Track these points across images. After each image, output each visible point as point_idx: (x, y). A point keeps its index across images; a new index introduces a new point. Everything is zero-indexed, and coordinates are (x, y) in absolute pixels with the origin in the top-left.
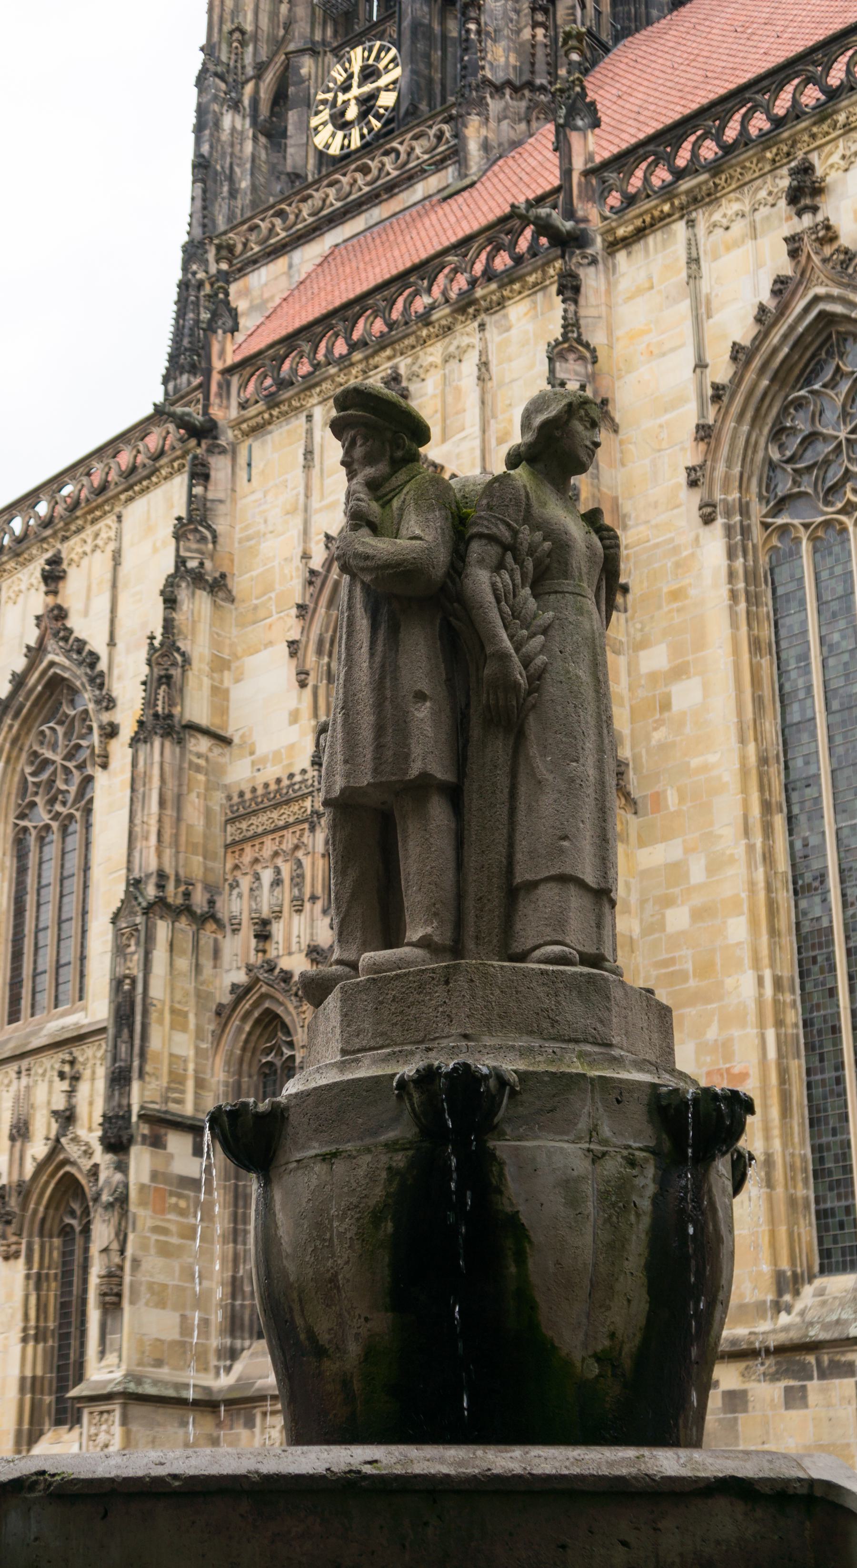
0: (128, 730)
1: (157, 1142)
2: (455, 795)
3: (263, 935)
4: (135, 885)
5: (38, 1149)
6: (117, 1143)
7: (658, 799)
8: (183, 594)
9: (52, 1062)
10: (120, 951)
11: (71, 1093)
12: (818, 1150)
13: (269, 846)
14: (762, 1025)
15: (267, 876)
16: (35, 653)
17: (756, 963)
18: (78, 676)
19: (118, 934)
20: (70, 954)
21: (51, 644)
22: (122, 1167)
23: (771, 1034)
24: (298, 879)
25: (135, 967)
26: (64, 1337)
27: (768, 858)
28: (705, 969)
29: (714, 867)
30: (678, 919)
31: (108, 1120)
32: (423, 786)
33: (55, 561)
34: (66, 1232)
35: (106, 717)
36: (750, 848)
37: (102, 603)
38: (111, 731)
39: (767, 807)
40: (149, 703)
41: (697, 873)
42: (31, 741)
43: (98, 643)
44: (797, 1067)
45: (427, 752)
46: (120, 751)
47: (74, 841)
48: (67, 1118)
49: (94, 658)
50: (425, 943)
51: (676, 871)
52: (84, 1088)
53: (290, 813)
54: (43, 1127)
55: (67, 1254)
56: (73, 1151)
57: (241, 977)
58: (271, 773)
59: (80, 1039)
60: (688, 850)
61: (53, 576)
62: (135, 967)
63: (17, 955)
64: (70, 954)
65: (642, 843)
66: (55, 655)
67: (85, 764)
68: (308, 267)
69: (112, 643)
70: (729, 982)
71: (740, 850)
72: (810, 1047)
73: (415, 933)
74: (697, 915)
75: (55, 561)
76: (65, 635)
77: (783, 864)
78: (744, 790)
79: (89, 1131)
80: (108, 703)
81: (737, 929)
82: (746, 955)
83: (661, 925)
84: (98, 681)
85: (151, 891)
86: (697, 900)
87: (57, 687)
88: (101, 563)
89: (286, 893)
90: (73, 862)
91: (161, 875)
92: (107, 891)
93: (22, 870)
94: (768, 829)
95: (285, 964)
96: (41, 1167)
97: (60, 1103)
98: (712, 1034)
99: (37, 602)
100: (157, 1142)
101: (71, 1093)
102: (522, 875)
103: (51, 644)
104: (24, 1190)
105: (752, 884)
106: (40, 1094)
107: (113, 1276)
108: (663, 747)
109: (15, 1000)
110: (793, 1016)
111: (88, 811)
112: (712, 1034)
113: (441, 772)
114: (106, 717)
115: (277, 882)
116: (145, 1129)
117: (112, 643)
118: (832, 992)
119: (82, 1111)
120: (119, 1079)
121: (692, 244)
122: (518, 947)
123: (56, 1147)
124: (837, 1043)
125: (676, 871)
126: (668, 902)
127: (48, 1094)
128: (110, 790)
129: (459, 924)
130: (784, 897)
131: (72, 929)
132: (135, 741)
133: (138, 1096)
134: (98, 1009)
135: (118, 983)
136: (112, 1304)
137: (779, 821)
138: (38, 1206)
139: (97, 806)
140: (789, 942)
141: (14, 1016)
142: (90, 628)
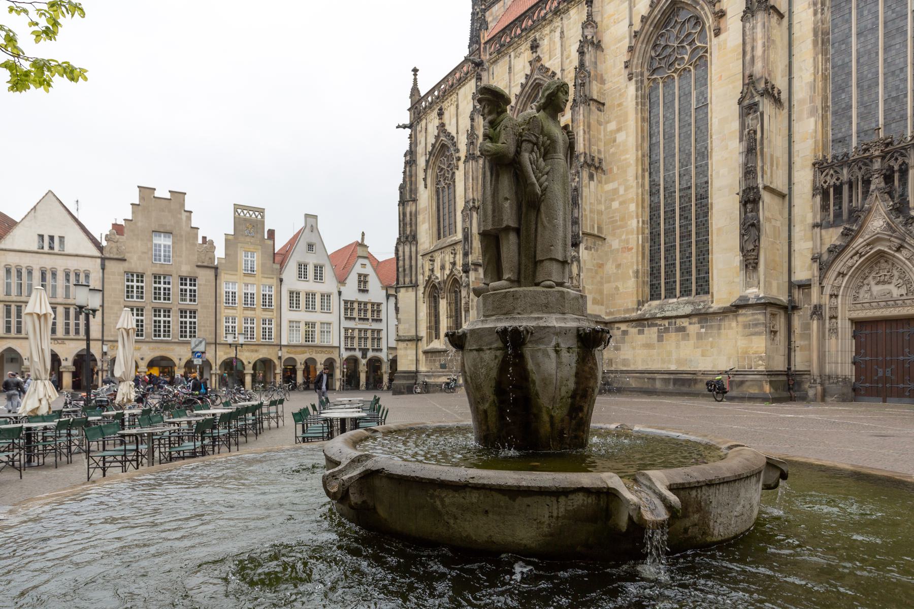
0: (463, 159)
1: (476, 270)
2: (518, 231)
4: (467, 202)
5: (447, 272)
6: (466, 271)
7: (611, 169)
8: (476, 117)
9: (449, 250)
10: (464, 221)
11: (454, 258)
14: (638, 234)
16: (437, 137)
17: (637, 217)
18: (449, 143)
19: (463, 216)
20: (453, 221)
21: (441, 134)
22: (468, 277)
23: (640, 237)
25: (468, 225)
26: (457, 317)
27: (643, 185)
28: (623, 219)
29: (626, 190)
30: (615, 205)
31: (463, 265)
32: (508, 229)
33: (441, 109)
34: (455, 292)
35: (457, 155)
36: (638, 183)
37: (454, 121)
38: (459, 159)
39: (643, 170)
40: (468, 150)
41: (622, 191)
42: (438, 163)
43: (454, 133)
44: (647, 245)
45: (509, 219)
46: (461, 164)
47: (452, 190)
48: (454, 264)
49: (453, 137)
50: (508, 280)
51: (615, 191)
52: (458, 256)
54: (448, 266)
55: (456, 297)
56: (456, 272)
59: (456, 243)
61: (441, 114)
62: (468, 225)
63: (439, 222)
64: (453, 221)
65: (606, 183)
67: (453, 168)
69: (457, 133)
70: (629, 222)
71: (634, 184)
72: (651, 240)
73: (506, 276)
74: (621, 204)
75: (441, 109)
76: (445, 131)
77: (647, 187)
78: (637, 166)
79: (459, 267)
80: (458, 151)
81: (632, 207)
82: (634, 214)
83: (611, 207)
84: (454, 144)
85: (471, 204)
86: (621, 199)
87: (443, 146)
90: (452, 196)
91: (474, 199)
92: (460, 204)
93: (438, 199)
94: (643, 177)
96: (448, 276)
97: (452, 261)
98: (624, 237)
99: (437, 122)
100: (476, 270)
101: (454, 258)
102: (539, 258)
103: (441, 134)
104: (445, 282)
105: (637, 193)
106: (447, 258)
107: (467, 303)
108: (613, 154)
109: (439, 234)
110: (647, 231)
111: (454, 182)
112: (624, 237)
113: (513, 224)
114: (457, 155)
116: (473, 267)
117: (457, 133)
118: (659, 224)
119: (457, 262)
120: (466, 255)
122: (537, 281)
123: (452, 271)
124: (660, 238)
125: (615, 191)
126: (613, 200)
127: (449, 258)
128: (459, 175)
129: (519, 273)
130: (647, 197)
131: (453, 214)
132: (465, 162)
133: (470, 259)
134: (459, 236)
135: (464, 229)
136: (467, 311)
137: (647, 174)
138: (448, 285)
140: (647, 210)
141: (439, 238)
142: (451, 129)
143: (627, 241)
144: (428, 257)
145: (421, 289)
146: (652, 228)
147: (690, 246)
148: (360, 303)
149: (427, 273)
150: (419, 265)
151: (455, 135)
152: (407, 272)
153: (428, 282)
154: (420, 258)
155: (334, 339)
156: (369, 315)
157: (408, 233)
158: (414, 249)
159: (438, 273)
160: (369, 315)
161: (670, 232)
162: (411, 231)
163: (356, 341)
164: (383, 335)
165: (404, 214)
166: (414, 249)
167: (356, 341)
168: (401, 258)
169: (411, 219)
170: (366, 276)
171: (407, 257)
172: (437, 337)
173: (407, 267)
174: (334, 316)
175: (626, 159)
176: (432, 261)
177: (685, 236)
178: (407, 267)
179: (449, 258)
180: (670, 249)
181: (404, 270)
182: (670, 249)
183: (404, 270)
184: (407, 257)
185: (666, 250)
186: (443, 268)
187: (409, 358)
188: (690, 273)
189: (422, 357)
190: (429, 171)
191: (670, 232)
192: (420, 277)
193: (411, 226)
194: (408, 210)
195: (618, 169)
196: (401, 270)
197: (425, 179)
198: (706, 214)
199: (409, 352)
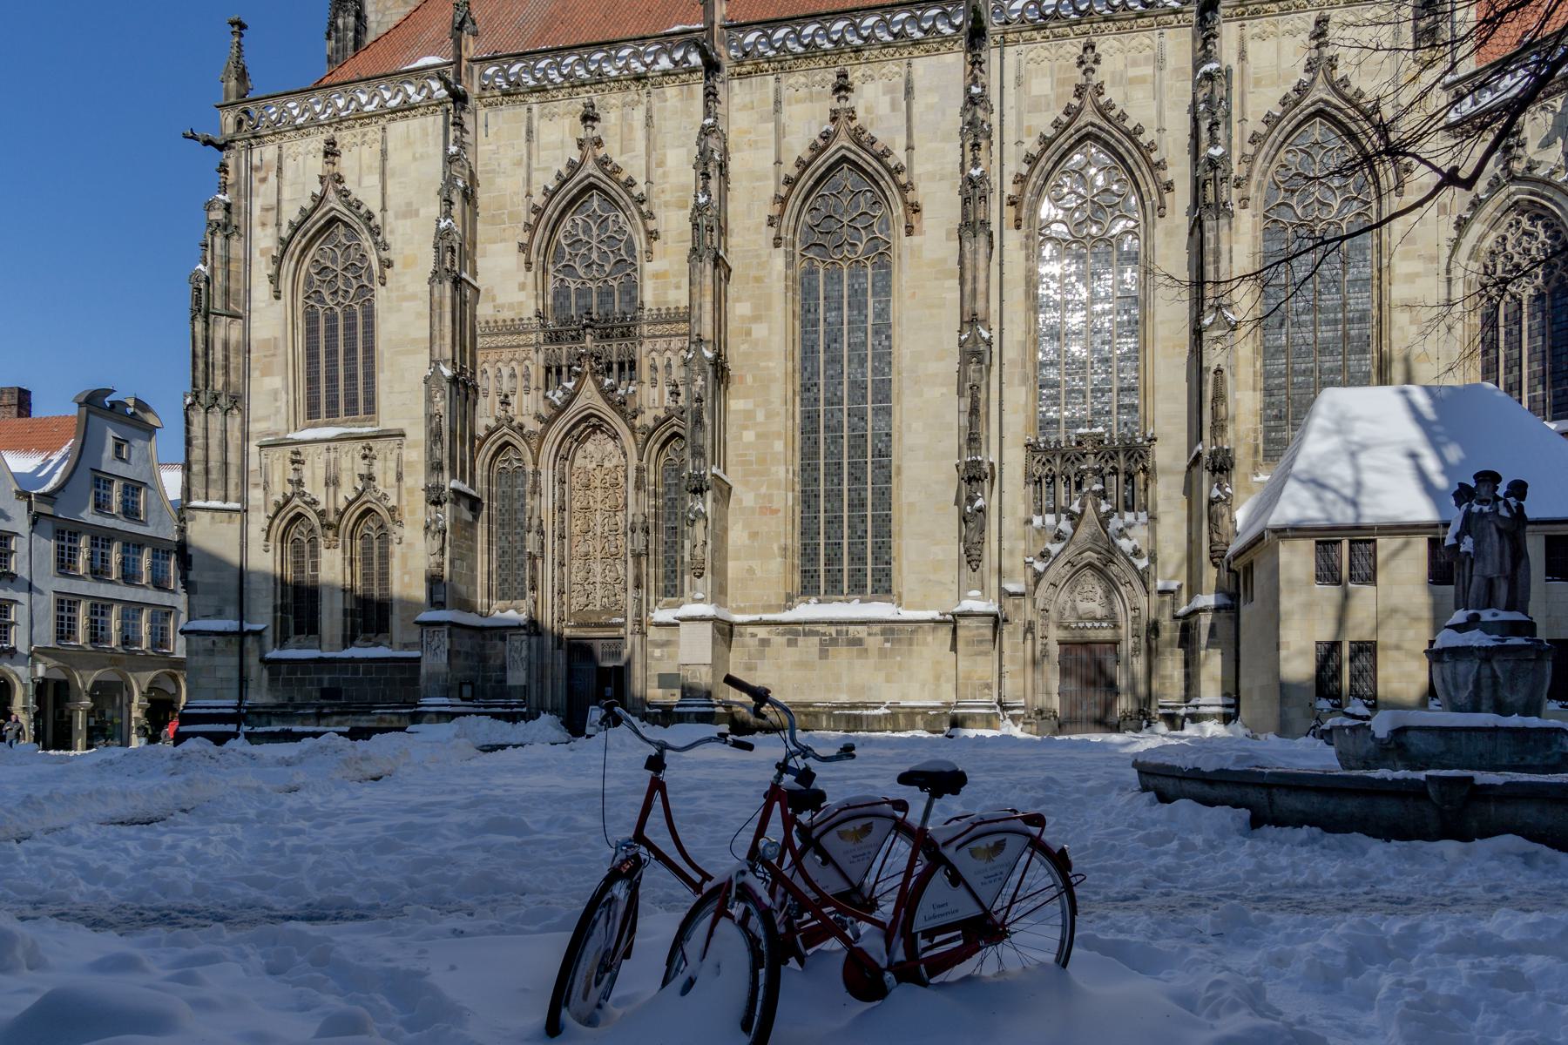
3: (505, 403)
5: (346, 492)
9: (359, 445)
12: (805, 546)
13: (506, 355)
15: (506, 372)
16: (319, 200)
24: (527, 377)
29: (768, 416)
37: (373, 180)
41: (760, 417)
43: (372, 204)
49: (370, 216)
53: (516, 340)
58: (507, 315)
60: (756, 405)
70: (774, 469)
74: (758, 436)
81: (779, 446)
88: (369, 155)
89: (520, 382)
110: (798, 488)
112: (763, 490)
126: (746, 428)
138: (348, 522)
143: (770, 497)
146: (805, 483)
147: (864, 521)
150: (254, 464)
151: (376, 210)
154: (253, 448)
161: (834, 495)
162: (227, 384)
168: (198, 442)
173: (214, 463)
175: (768, 368)
177: (858, 504)
178: (214, 463)
180: (834, 521)
182: (834, 521)
185: (828, 522)
186: (332, 482)
188: (863, 560)
190: (288, 266)
191: (834, 495)
192: (256, 495)
193: (227, 373)
195: (755, 380)
196: (196, 468)
197: (275, 279)
199: (218, 660)
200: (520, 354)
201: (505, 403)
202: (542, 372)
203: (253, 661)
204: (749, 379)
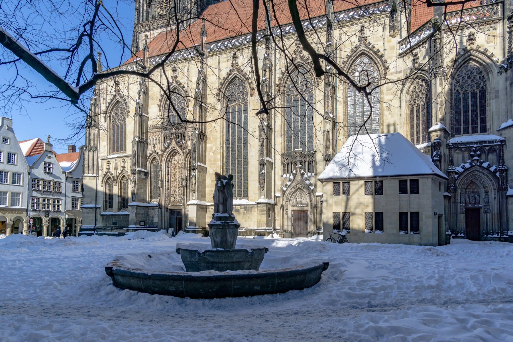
3: (154, 147)
15: (155, 138)
24: (159, 140)
52: (126, 164)
57: (151, 152)
66: (118, 97)
68: (156, 35)
76: (120, 94)
84: (126, 103)
89: (158, 141)
95: (157, 151)
96: (120, 174)
106: (119, 164)
112: (215, 168)
114: (128, 109)
115: (156, 140)
121: (219, 60)
127: (120, 164)
139: (127, 122)
144: (106, 161)
145: (100, 179)
148: (44, 182)
149: (105, 170)
152: (91, 167)
153: (105, 175)
155: (23, 203)
156: (51, 189)
157: (92, 145)
158: (95, 154)
159: (112, 171)
160: (51, 189)
162: (94, 144)
163: (40, 206)
164: (62, 202)
165: (90, 134)
166: (95, 154)
167: (40, 206)
169: (94, 138)
170: (50, 164)
171: (91, 159)
172: (111, 206)
173: (90, 164)
174: (23, 188)
176: (109, 163)
178: (90, 164)
179: (120, 164)
181: (89, 167)
183: (89, 167)
184: (91, 159)
186: (116, 168)
187: (90, 218)
189: (99, 218)
192: (100, 172)
194: (92, 132)
198: (247, 165)
199: (90, 215)
200: (158, 134)
201: (154, 147)
202: (163, 138)
203: (98, 215)
204: (212, 138)
